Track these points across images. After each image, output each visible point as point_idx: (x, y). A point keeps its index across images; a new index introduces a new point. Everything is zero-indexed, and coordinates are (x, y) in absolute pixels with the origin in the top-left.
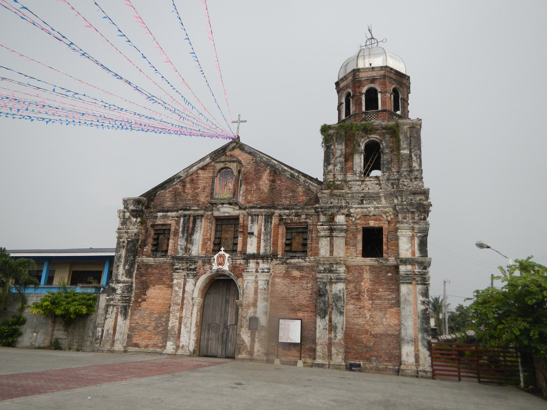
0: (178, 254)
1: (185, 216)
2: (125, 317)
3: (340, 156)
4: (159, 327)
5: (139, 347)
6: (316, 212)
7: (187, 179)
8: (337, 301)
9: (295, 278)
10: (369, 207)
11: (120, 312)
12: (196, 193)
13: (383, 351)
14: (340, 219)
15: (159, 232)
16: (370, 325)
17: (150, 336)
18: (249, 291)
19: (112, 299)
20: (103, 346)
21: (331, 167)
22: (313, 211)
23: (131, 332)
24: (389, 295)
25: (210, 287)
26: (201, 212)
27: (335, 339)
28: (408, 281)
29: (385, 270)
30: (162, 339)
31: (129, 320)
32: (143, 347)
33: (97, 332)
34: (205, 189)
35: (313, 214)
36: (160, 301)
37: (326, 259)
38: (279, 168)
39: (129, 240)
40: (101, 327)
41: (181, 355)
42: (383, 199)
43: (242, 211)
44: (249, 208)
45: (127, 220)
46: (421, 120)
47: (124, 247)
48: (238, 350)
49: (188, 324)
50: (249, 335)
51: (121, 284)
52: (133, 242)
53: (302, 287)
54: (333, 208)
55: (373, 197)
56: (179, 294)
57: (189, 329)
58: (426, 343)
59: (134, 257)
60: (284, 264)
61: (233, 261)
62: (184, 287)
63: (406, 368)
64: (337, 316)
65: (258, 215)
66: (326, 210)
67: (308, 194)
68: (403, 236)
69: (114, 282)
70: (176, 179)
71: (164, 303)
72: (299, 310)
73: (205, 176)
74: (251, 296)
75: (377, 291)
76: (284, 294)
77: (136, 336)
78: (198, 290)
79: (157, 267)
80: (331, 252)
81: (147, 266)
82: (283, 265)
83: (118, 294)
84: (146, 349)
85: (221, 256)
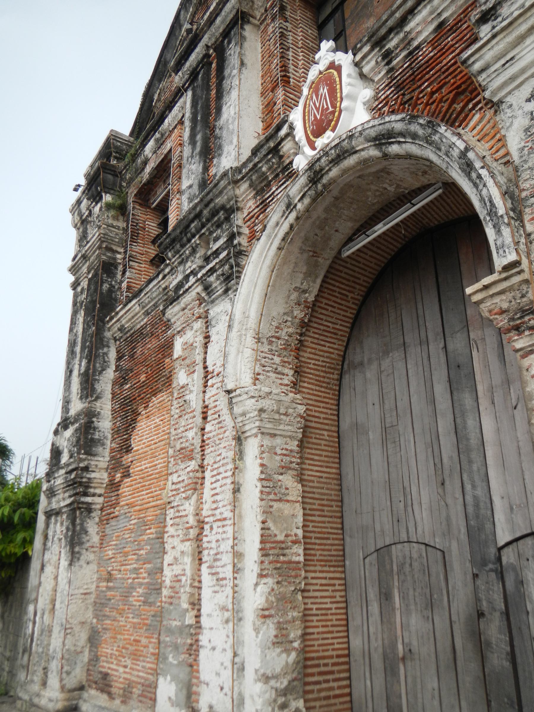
25: (352, 328)
31: (94, 567)
61: (388, 56)
78: (250, 341)
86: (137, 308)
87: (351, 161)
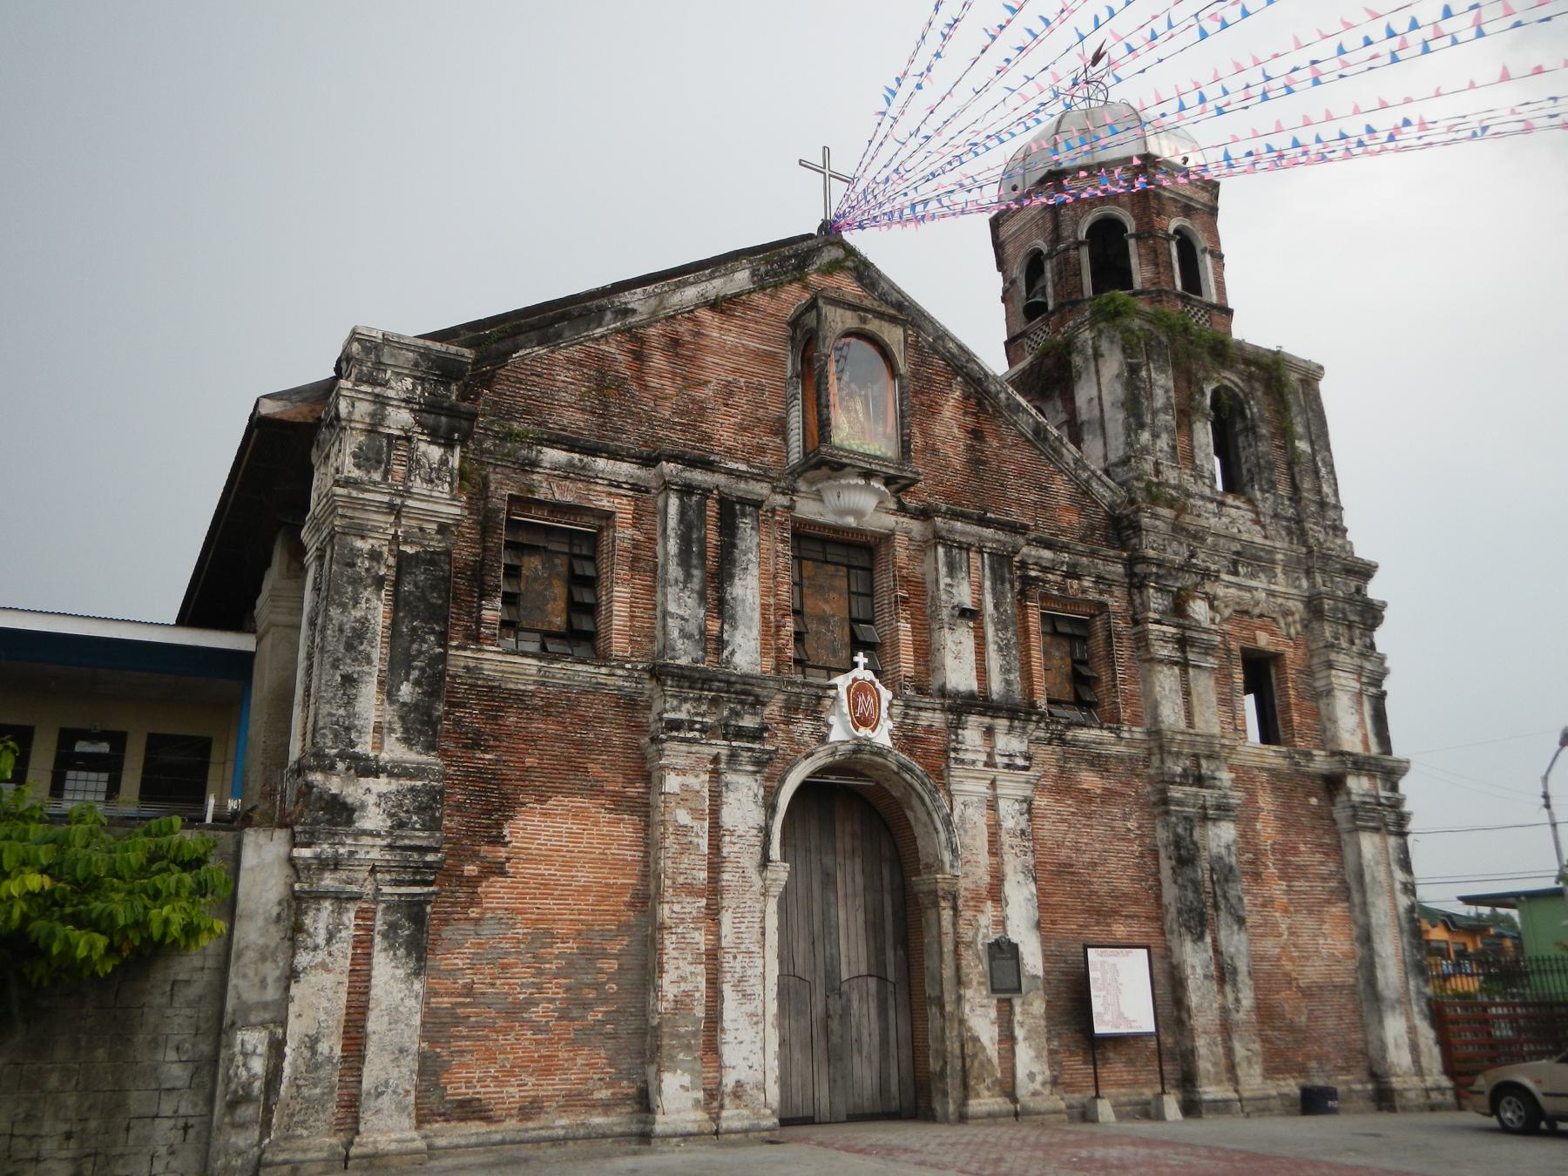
0: (672, 658)
1: (686, 490)
2: (419, 959)
3: (1165, 410)
4: (586, 1006)
5: (488, 1120)
6: (1130, 574)
7: (652, 331)
8: (1227, 880)
9: (1086, 797)
10: (1256, 589)
11: (385, 936)
12: (694, 401)
13: (1330, 1039)
14: (1199, 610)
15: (523, 538)
16: (1292, 959)
17: (544, 1052)
18: (974, 837)
19: (335, 864)
20: (287, 1139)
21: (1145, 436)
22: (1120, 569)
23: (433, 1042)
24: (1322, 864)
26: (761, 489)
27: (1238, 1011)
28: (1371, 824)
29: (1302, 786)
30: (610, 1066)
32: (512, 1116)
33: (240, 1058)
34: (731, 394)
35: (1116, 578)
36: (584, 876)
37: (1187, 738)
38: (998, 393)
39: (410, 550)
40: (263, 1025)
41: (746, 1131)
42: (1279, 570)
43: (906, 522)
44: (946, 513)
45: (389, 444)
46: (1321, 368)
47: (379, 582)
48: (958, 1081)
49: (752, 981)
50: (993, 1014)
51: (383, 779)
52: (432, 562)
53: (1113, 829)
54: (1188, 571)
55: (1259, 559)
56: (696, 840)
57: (761, 1004)
58: (1423, 1004)
59: (443, 639)
60: (1055, 742)
62: (715, 813)
63: (1405, 1086)
64: (1232, 933)
65: (968, 550)
66: (1171, 574)
67: (1083, 509)
68: (1344, 689)
69: (340, 766)
70: (609, 316)
71: (607, 885)
72: (1115, 912)
73: (730, 339)
74: (980, 858)
75: (1296, 852)
76: (1064, 852)
77: (467, 1058)
79: (549, 705)
80: (1189, 715)
81: (497, 698)
82: (1050, 748)
83: (370, 834)
84: (530, 1125)
85: (859, 689)
86: (534, 671)
87: (880, 760)
